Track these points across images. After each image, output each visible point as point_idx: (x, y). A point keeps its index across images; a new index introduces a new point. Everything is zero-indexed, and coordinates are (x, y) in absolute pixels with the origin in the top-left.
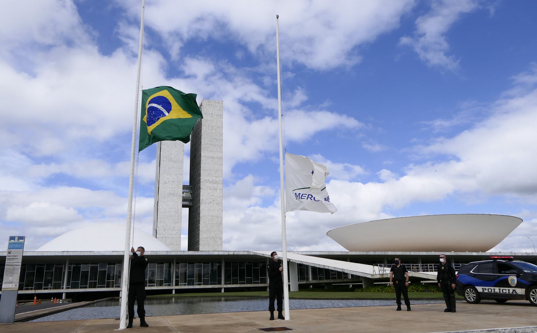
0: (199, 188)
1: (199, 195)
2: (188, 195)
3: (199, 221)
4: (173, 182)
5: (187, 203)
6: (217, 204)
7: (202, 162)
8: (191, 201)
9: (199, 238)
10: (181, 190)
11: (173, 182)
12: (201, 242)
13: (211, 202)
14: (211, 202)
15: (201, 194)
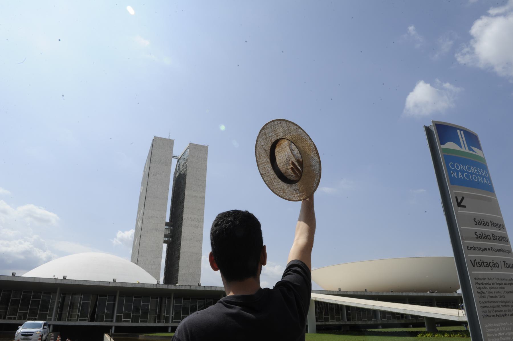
0: (181, 226)
1: (180, 232)
2: (168, 232)
3: (179, 257)
4: (157, 218)
5: (167, 239)
6: (197, 241)
7: (185, 200)
8: (171, 237)
9: (178, 273)
10: (164, 226)
11: (157, 218)
12: (180, 278)
13: (191, 239)
14: (191, 239)
15: (183, 230)
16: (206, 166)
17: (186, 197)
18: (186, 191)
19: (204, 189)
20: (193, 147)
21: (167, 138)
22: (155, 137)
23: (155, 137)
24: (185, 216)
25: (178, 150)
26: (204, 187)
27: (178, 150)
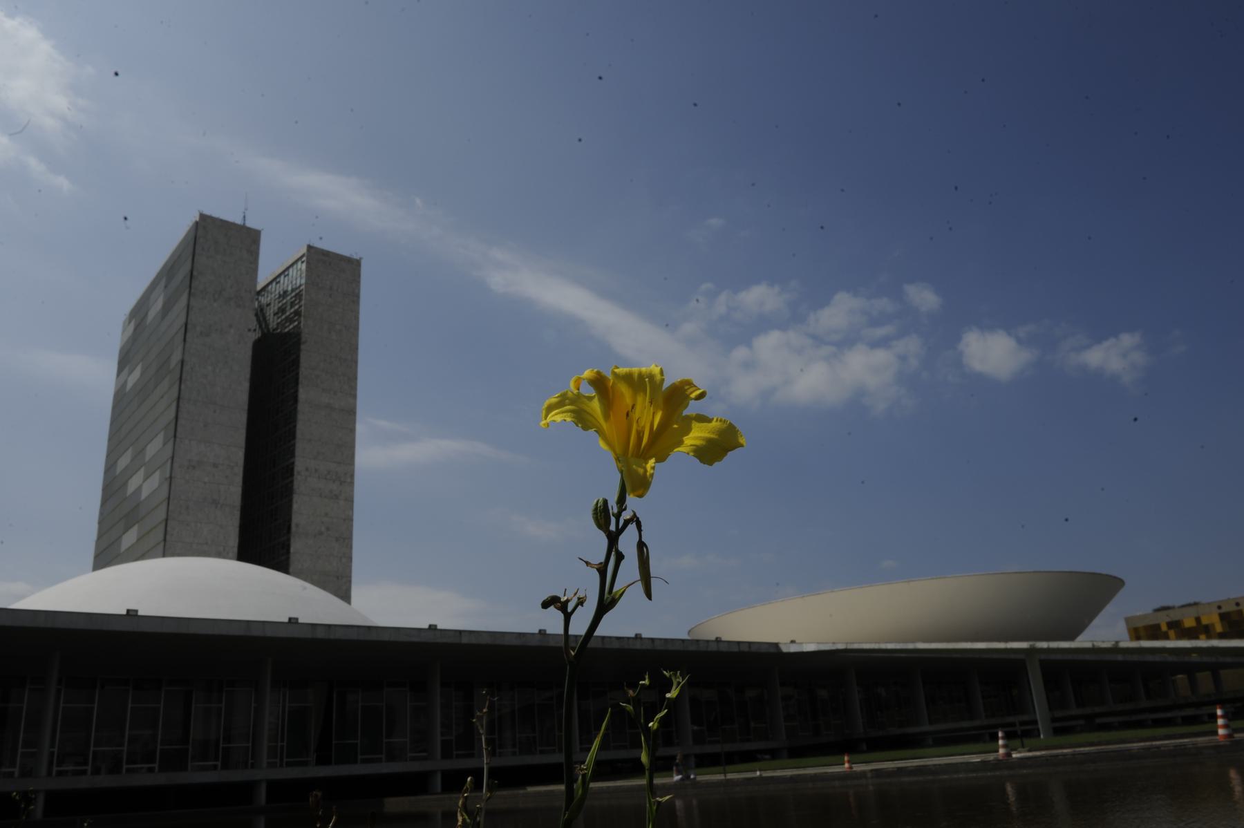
4: (215, 465)
6: (337, 540)
7: (300, 417)
11: (215, 465)
13: (321, 533)
14: (321, 533)
15: (295, 506)
16: (357, 318)
17: (302, 407)
18: (301, 390)
19: (354, 388)
20: (317, 258)
21: (239, 221)
22: (203, 216)
23: (203, 216)
24: (300, 464)
25: (276, 260)
26: (352, 379)
27: (276, 260)
